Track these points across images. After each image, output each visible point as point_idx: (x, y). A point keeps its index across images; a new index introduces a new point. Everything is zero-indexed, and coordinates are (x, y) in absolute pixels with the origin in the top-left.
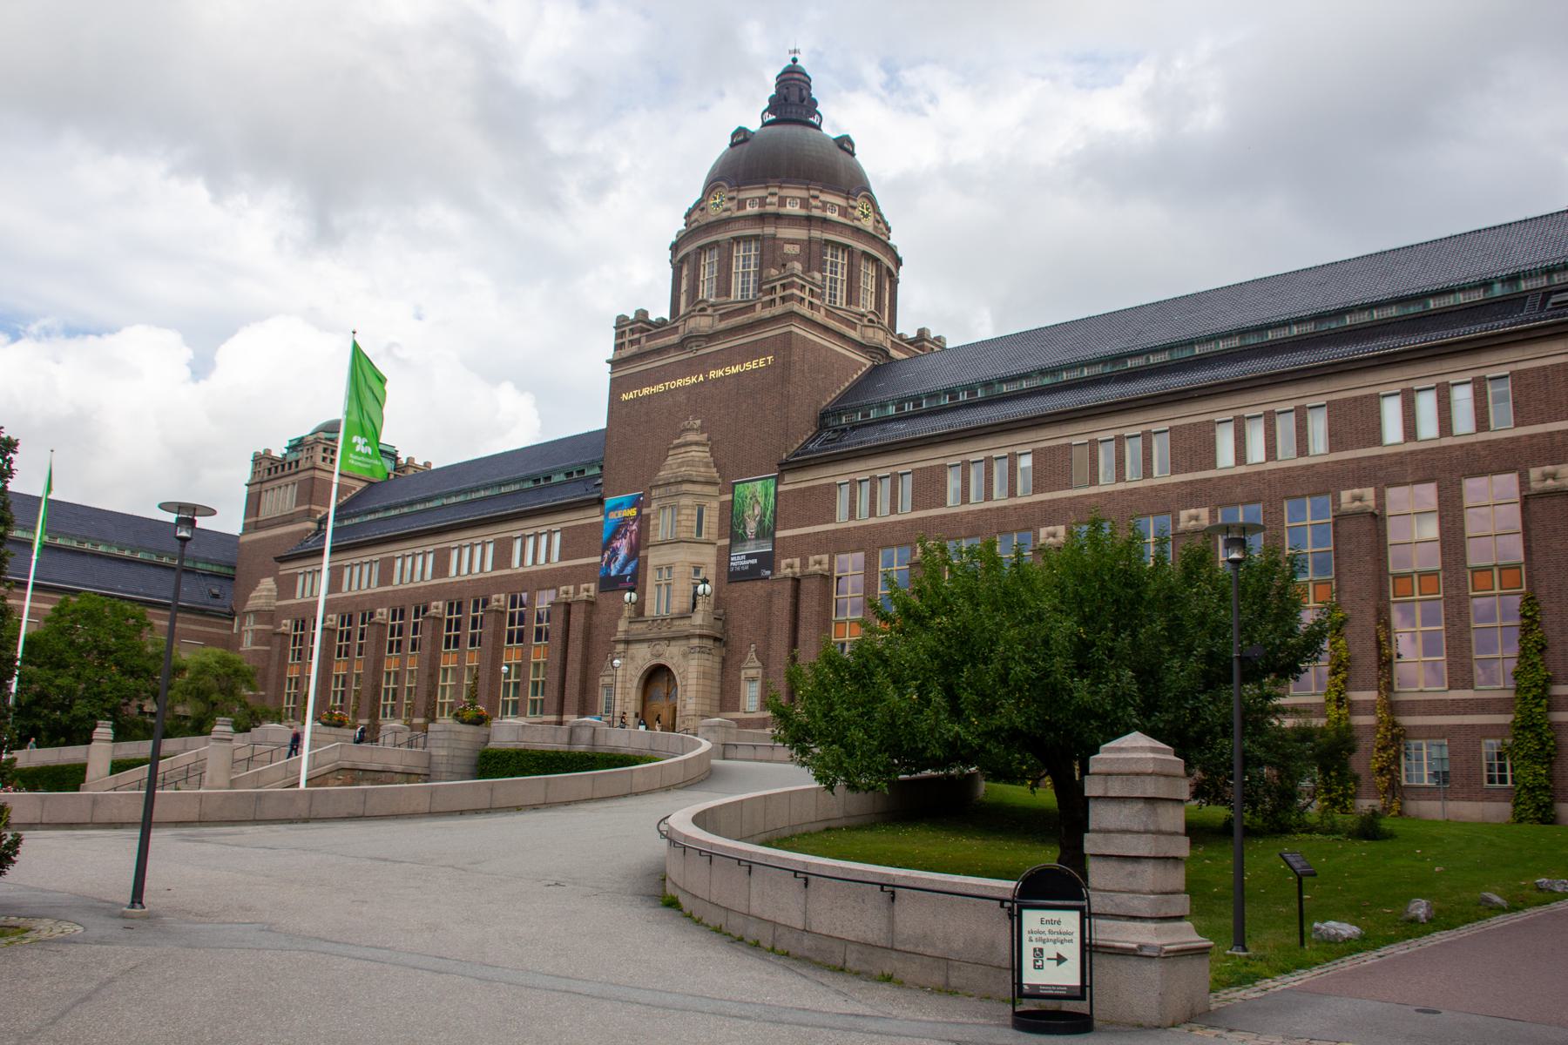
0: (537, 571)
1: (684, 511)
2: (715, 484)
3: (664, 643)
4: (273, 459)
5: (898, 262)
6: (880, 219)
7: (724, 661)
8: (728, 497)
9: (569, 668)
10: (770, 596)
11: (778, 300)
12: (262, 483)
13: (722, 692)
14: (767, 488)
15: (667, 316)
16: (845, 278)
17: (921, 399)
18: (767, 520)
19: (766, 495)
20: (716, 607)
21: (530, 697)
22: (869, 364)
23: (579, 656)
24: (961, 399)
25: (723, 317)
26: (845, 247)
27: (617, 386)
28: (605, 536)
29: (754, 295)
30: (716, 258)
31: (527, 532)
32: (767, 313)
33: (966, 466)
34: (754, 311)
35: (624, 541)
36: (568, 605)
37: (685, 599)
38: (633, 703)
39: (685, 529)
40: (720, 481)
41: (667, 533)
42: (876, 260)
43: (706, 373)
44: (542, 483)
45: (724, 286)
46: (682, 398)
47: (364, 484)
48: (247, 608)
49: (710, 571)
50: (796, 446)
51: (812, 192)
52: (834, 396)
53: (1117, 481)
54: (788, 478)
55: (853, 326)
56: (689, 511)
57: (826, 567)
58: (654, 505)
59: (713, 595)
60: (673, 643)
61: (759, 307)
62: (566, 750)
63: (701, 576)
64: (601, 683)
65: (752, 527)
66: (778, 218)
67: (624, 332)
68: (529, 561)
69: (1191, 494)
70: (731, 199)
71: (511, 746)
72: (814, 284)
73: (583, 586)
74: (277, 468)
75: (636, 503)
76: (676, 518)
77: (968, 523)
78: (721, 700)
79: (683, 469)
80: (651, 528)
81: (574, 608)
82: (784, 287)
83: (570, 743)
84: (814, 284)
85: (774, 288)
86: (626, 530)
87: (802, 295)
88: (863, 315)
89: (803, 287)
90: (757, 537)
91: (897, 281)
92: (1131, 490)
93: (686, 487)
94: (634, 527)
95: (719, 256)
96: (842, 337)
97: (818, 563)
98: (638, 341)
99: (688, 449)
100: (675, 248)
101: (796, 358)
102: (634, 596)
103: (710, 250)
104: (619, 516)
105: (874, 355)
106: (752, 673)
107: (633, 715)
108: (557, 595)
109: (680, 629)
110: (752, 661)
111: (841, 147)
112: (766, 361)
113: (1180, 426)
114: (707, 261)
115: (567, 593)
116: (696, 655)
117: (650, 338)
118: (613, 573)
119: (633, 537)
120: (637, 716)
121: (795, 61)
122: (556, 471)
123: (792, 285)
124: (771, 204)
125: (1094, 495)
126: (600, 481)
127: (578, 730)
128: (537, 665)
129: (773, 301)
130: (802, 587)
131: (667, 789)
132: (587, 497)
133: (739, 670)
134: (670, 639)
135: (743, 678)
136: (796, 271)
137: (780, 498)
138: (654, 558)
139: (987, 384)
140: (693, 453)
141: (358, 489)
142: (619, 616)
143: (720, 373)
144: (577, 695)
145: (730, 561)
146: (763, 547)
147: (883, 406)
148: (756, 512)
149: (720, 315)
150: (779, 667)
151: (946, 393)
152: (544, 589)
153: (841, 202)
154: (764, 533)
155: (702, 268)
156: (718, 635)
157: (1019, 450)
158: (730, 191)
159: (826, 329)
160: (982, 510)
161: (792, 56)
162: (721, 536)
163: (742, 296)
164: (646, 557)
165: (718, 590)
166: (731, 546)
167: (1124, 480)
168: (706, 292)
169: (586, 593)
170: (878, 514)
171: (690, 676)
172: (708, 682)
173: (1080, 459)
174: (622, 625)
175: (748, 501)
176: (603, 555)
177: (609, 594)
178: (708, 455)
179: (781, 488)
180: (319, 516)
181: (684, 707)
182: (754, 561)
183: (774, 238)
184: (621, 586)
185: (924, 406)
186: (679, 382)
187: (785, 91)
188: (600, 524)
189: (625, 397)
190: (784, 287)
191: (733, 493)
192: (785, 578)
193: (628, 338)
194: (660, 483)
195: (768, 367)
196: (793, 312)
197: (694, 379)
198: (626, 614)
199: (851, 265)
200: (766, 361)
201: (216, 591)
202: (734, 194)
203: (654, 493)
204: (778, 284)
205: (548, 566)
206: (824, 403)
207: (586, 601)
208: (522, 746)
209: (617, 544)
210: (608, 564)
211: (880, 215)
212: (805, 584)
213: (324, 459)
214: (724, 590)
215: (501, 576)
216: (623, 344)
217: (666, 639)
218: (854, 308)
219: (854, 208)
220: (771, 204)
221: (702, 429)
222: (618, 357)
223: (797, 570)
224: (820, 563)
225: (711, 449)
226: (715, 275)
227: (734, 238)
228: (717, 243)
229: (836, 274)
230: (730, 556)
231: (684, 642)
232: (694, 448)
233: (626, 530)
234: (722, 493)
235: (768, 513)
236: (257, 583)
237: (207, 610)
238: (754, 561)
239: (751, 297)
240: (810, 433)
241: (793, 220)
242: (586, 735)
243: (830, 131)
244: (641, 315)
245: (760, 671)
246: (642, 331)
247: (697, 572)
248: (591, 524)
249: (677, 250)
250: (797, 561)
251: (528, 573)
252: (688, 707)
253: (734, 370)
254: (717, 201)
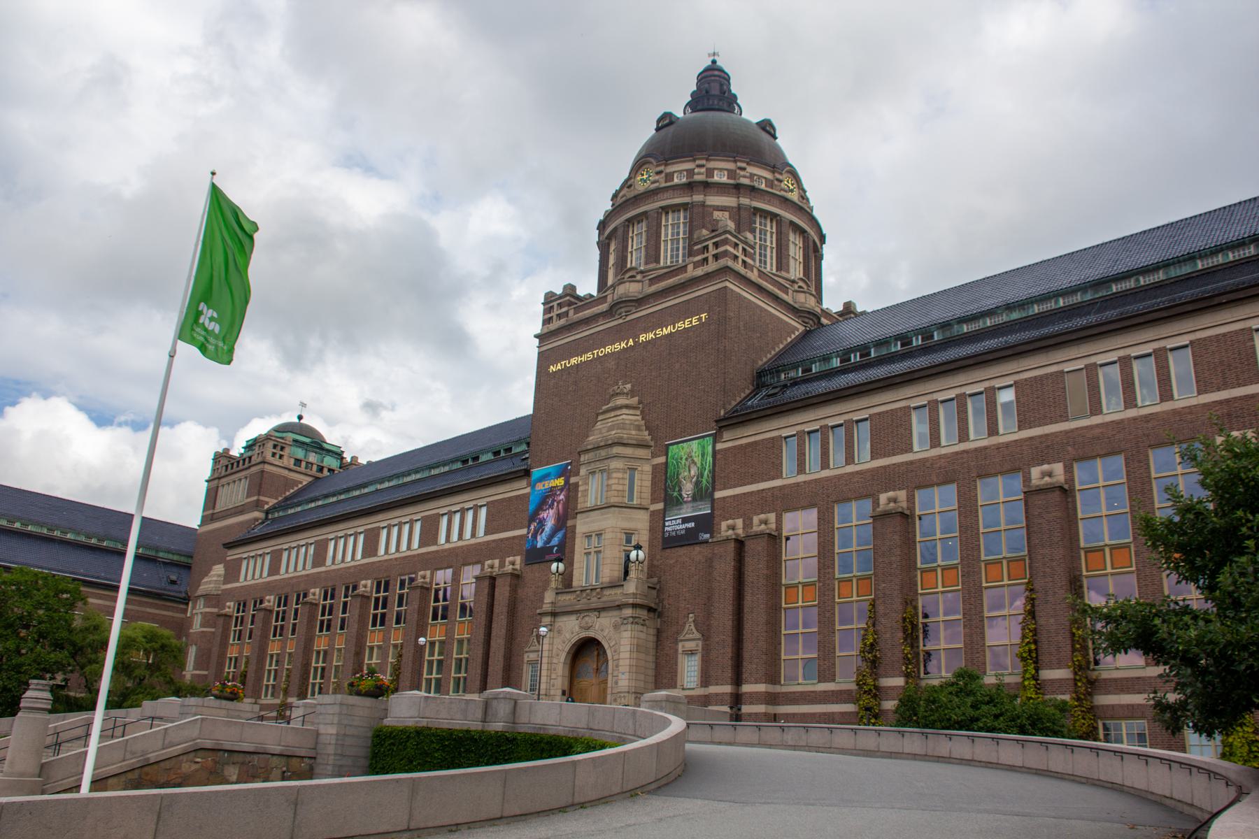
0: (462, 547)
1: (615, 475)
2: (647, 446)
3: (593, 615)
4: (231, 457)
5: (822, 238)
6: (804, 197)
7: (659, 633)
8: (662, 460)
9: (493, 643)
10: (710, 562)
11: (710, 259)
12: (219, 478)
13: (658, 666)
14: (703, 447)
15: (595, 293)
16: (774, 245)
17: (870, 348)
18: (704, 481)
19: (703, 455)
20: (650, 576)
21: (453, 675)
22: (801, 329)
23: (504, 631)
24: (914, 344)
25: (653, 281)
26: (774, 216)
27: (544, 359)
28: (532, 507)
29: (684, 261)
30: (644, 229)
31: (454, 508)
32: (700, 272)
33: (933, 406)
34: (686, 272)
35: (551, 512)
36: (493, 579)
37: (616, 567)
38: (560, 680)
39: (616, 493)
40: (652, 443)
41: (596, 498)
42: (802, 232)
43: (636, 337)
44: (470, 463)
45: (653, 253)
46: (611, 364)
47: (310, 479)
48: (199, 593)
49: (643, 537)
50: (734, 403)
51: (739, 164)
52: (769, 356)
53: (1126, 408)
54: (727, 435)
55: (785, 290)
56: (620, 475)
57: (773, 526)
58: (583, 471)
59: (646, 563)
60: (603, 614)
61: (690, 267)
62: (480, 728)
63: (633, 543)
64: (526, 659)
65: (688, 489)
66: (707, 186)
67: (552, 307)
68: (455, 536)
69: (1229, 415)
70: (659, 173)
71: (410, 723)
72: (746, 243)
73: (508, 560)
74: (233, 464)
75: (564, 472)
76: (605, 483)
77: (940, 468)
78: (656, 676)
79: (614, 432)
80: (579, 495)
81: (499, 582)
82: (716, 245)
83: (484, 721)
84: (746, 243)
85: (706, 248)
86: (554, 501)
87: (735, 252)
88: (793, 282)
89: (736, 245)
90: (694, 499)
91: (821, 258)
92: (1146, 416)
93: (616, 450)
94: (562, 497)
95: (648, 227)
96: (776, 298)
97: (763, 522)
98: (567, 313)
99: (618, 412)
100: (602, 226)
101: (732, 314)
102: (561, 566)
103: (638, 223)
104: (546, 486)
105: (807, 320)
106: (690, 645)
107: (560, 692)
108: (482, 569)
109: (610, 598)
110: (690, 632)
111: (764, 129)
112: (700, 319)
113: (1205, 339)
114: (635, 233)
115: (492, 567)
116: (629, 626)
117: (577, 310)
118: (540, 544)
119: (560, 506)
120: (564, 693)
121: (714, 62)
122: (484, 451)
123: (726, 242)
124: (699, 174)
125: (1097, 426)
126: (527, 455)
127: (495, 703)
128: (461, 642)
129: (706, 260)
130: (747, 548)
131: (632, 794)
132: (513, 470)
133: (676, 642)
134: (600, 610)
135: (680, 650)
136: (728, 229)
137: (718, 456)
138: (582, 525)
139: (945, 326)
140: (624, 417)
141: (304, 483)
142: (545, 589)
143: (651, 335)
144: (501, 673)
145: (664, 526)
146: (700, 510)
147: (826, 359)
148: (692, 473)
149: (650, 279)
150: (722, 637)
151: (896, 340)
152: (469, 564)
153: (769, 175)
154: (701, 494)
155: (629, 255)
156: (653, 605)
157: (998, 383)
158: (657, 166)
159: (760, 289)
160: (957, 453)
161: (712, 58)
162: (654, 501)
163: (672, 262)
164: (574, 527)
165: (651, 556)
166: (665, 510)
167: (1136, 406)
168: (635, 259)
169: (511, 567)
170: (831, 466)
171: (622, 649)
172: (642, 656)
173: (1076, 390)
174: (549, 597)
175: (684, 461)
176: (529, 526)
177: (536, 566)
178: (640, 418)
179: (719, 446)
180: (266, 507)
181: (616, 683)
182: (692, 525)
183: (703, 205)
184: (548, 557)
185: (873, 355)
186: (608, 349)
187: (707, 85)
188: (527, 496)
189: (552, 369)
190: (716, 245)
191: (667, 455)
192: (728, 539)
193: (556, 311)
194: (589, 447)
195: (702, 325)
196: (727, 267)
197: (623, 345)
198: (553, 585)
199: (780, 235)
200: (700, 319)
201: (174, 578)
202: (662, 168)
203: (583, 458)
204: (710, 243)
205: (473, 541)
206: (760, 363)
207: (512, 574)
208: (424, 723)
209: (544, 515)
210: (535, 536)
211: (805, 191)
212: (750, 546)
213: (274, 455)
214: (658, 557)
216: (551, 318)
217: (595, 610)
218: (784, 274)
219: (781, 181)
220: (699, 174)
221: (632, 393)
222: (546, 331)
223: (740, 531)
224: (766, 522)
225: (642, 412)
226: (644, 244)
227: (662, 208)
228: (645, 214)
229: (765, 241)
230: (665, 521)
231: (616, 613)
232: (625, 411)
233: (554, 501)
234: (654, 455)
235: (706, 473)
236: (210, 570)
237: (164, 595)
238: (692, 525)
239: (680, 262)
240: (747, 392)
241: (721, 188)
242: (503, 709)
243: (751, 113)
244: (570, 290)
245: (700, 643)
246: (570, 304)
247: (629, 541)
248: (517, 497)
249: (604, 227)
250: (739, 523)
251: (454, 549)
252: (621, 683)
253: (666, 331)
254: (645, 177)
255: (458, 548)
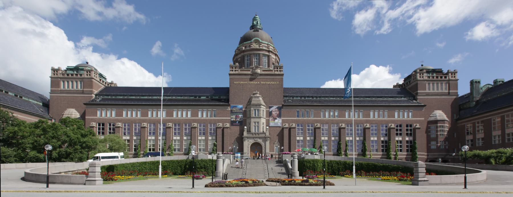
25: (264, 71)
40: (266, 106)
141: (103, 87)
162: (266, 117)
215: (195, 119)
255: (207, 119)
